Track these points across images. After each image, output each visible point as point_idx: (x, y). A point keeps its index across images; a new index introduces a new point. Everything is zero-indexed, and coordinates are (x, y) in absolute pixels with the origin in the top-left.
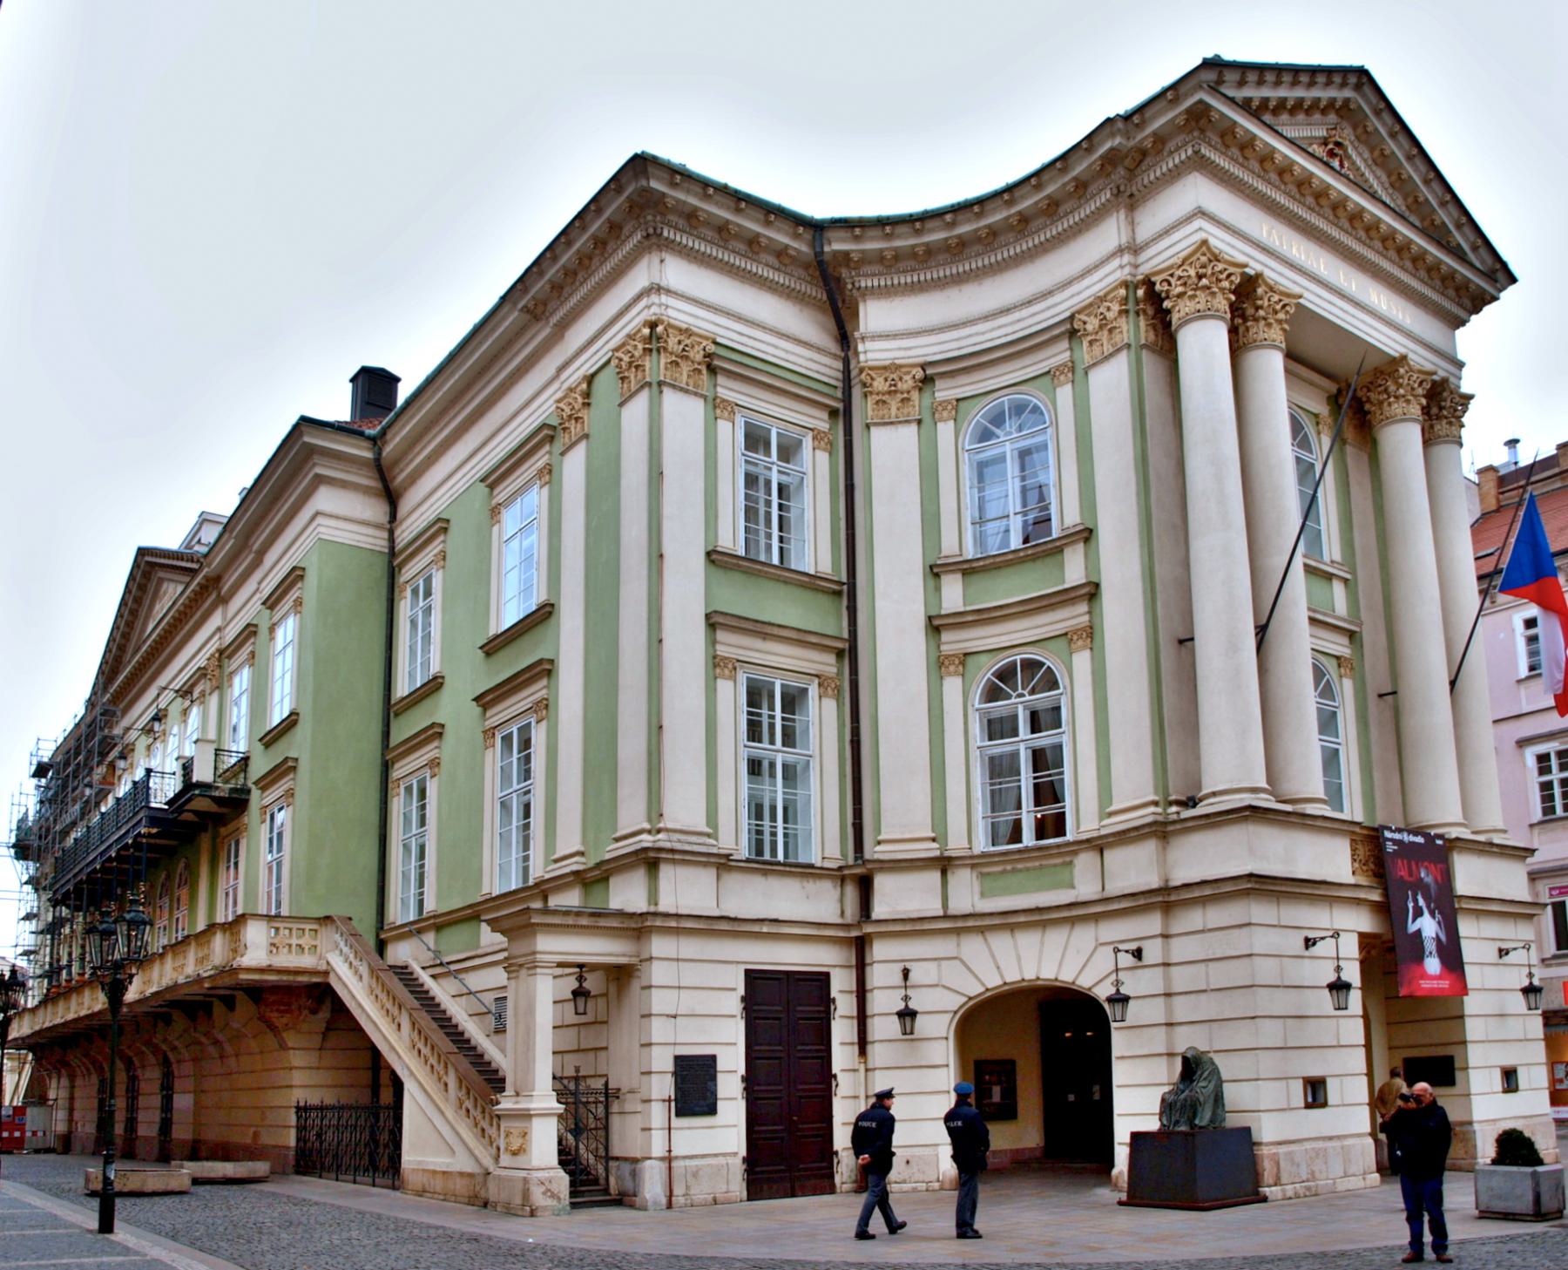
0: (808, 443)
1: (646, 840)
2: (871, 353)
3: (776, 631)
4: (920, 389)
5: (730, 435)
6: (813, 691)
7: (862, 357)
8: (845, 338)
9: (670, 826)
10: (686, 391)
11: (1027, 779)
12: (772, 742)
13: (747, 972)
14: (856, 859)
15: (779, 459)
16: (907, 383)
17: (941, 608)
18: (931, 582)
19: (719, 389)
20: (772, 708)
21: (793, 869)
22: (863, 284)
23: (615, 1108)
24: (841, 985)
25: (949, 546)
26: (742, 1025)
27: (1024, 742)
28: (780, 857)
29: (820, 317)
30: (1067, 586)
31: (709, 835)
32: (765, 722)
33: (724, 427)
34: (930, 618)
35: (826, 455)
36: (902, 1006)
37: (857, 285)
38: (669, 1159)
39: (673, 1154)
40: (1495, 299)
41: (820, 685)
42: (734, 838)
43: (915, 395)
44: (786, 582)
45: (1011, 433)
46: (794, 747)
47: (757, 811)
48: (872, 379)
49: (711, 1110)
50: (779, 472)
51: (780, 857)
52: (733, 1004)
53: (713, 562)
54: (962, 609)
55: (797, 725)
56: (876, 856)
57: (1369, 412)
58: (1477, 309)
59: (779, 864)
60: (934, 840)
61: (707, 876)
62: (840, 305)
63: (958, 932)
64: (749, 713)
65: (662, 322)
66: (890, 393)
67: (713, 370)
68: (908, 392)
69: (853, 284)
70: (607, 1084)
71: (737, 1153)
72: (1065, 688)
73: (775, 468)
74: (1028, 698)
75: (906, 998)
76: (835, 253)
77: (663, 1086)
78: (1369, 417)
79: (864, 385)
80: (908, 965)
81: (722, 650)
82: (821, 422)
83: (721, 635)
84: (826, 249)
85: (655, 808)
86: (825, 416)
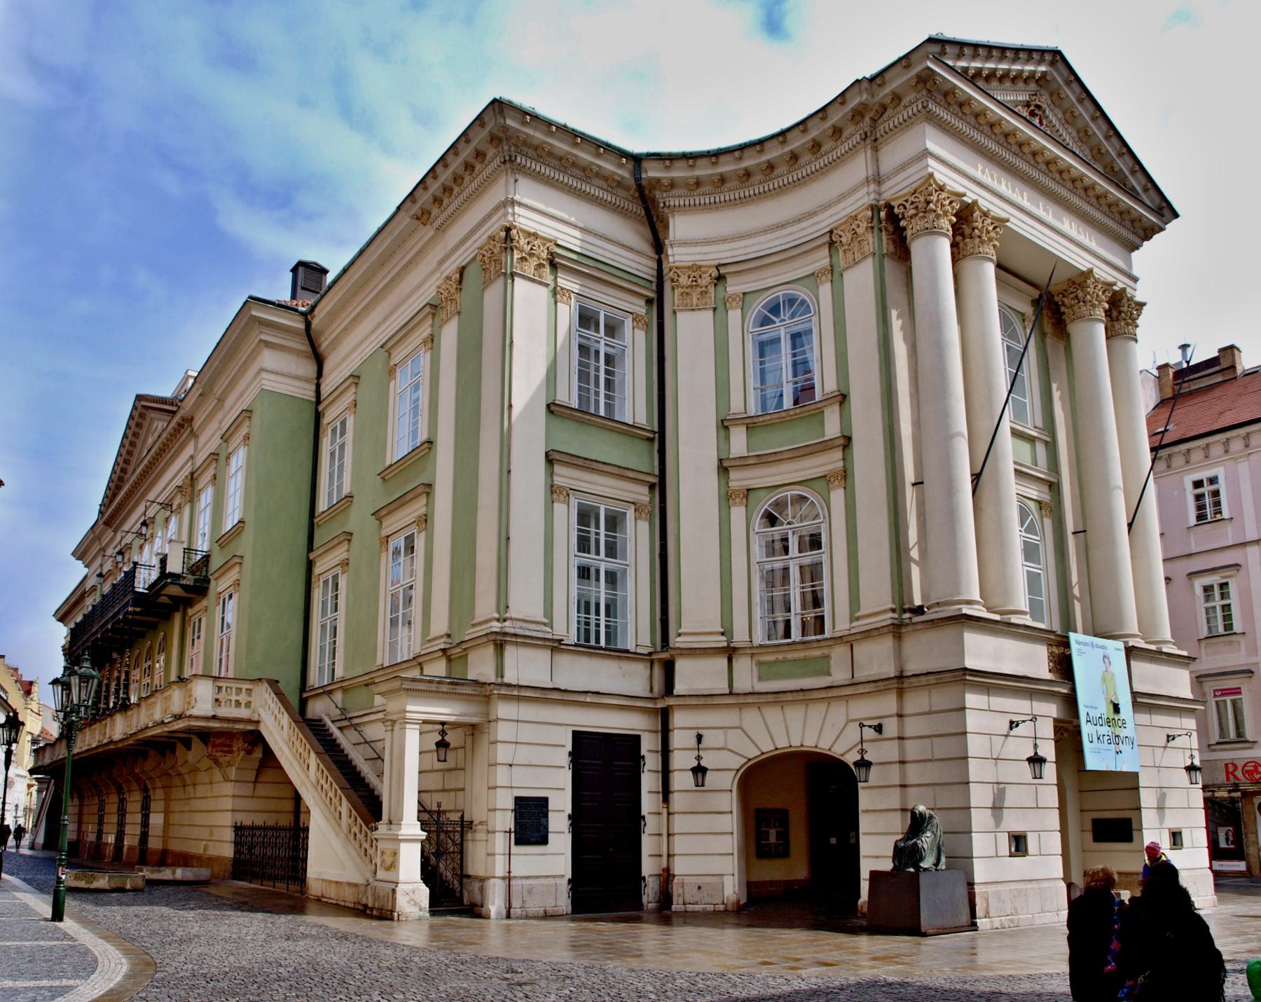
0: (628, 323)
1: (496, 626)
2: (677, 256)
3: (601, 467)
4: (715, 285)
5: (567, 313)
6: (630, 514)
7: (671, 259)
8: (659, 246)
9: (513, 616)
10: (533, 281)
11: (795, 590)
12: (598, 553)
13: (574, 733)
14: (663, 647)
15: (606, 335)
16: (705, 280)
17: (729, 453)
18: (722, 433)
19: (559, 280)
20: (597, 527)
21: (612, 653)
22: (672, 204)
23: (469, 836)
24: (649, 745)
25: (736, 405)
26: (569, 774)
27: (796, 559)
28: (603, 643)
29: (641, 228)
30: (826, 439)
31: (545, 624)
32: (593, 537)
34: (720, 461)
35: (644, 333)
36: (695, 764)
37: (667, 204)
38: (508, 878)
39: (511, 874)
40: (1162, 229)
42: (566, 627)
43: (711, 289)
44: (611, 430)
45: (785, 320)
46: (616, 558)
47: (585, 606)
48: (678, 276)
49: (544, 841)
50: (606, 345)
51: (603, 643)
52: (563, 758)
53: (552, 412)
54: (746, 455)
55: (618, 540)
56: (677, 645)
57: (1064, 313)
58: (1147, 237)
59: (601, 648)
60: (723, 634)
61: (545, 655)
62: (655, 219)
63: (740, 706)
64: (579, 530)
65: (515, 227)
66: (691, 287)
67: (554, 266)
68: (707, 287)
69: (664, 203)
70: (462, 817)
71: (563, 876)
72: (824, 518)
73: (602, 342)
75: (699, 758)
76: (650, 180)
77: (506, 821)
78: (1064, 317)
79: (672, 280)
80: (701, 732)
81: (558, 480)
82: (639, 307)
83: (558, 469)
84: (644, 176)
85: (503, 602)
86: (643, 303)
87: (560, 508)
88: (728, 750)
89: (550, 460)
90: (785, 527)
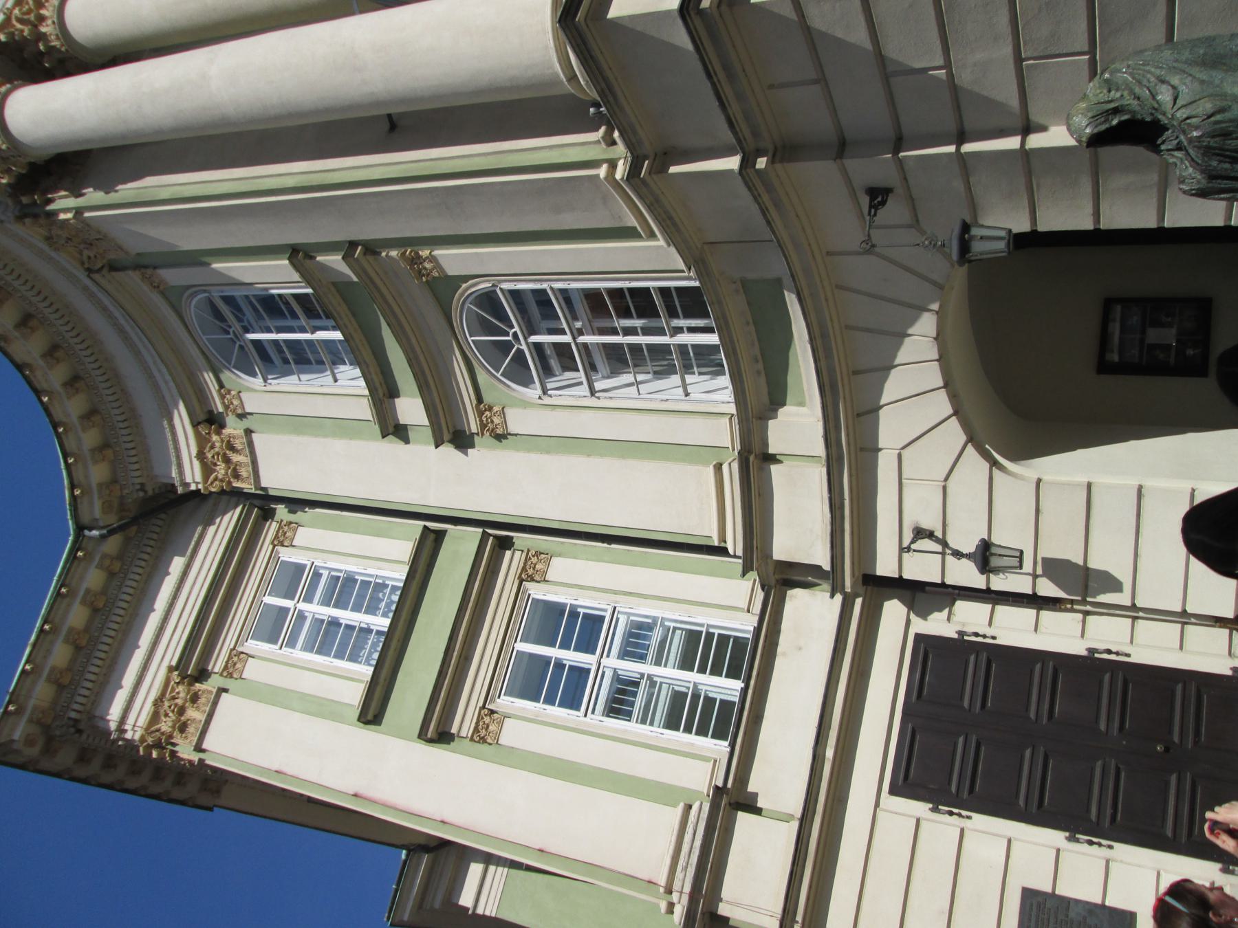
13: (894, 791)
33: (252, 670)
41: (531, 579)
50: (308, 599)
73: (302, 606)
74: (516, 329)
81: (467, 730)
87: (512, 734)
88: (946, 479)
89: (443, 737)
90: (524, 347)
